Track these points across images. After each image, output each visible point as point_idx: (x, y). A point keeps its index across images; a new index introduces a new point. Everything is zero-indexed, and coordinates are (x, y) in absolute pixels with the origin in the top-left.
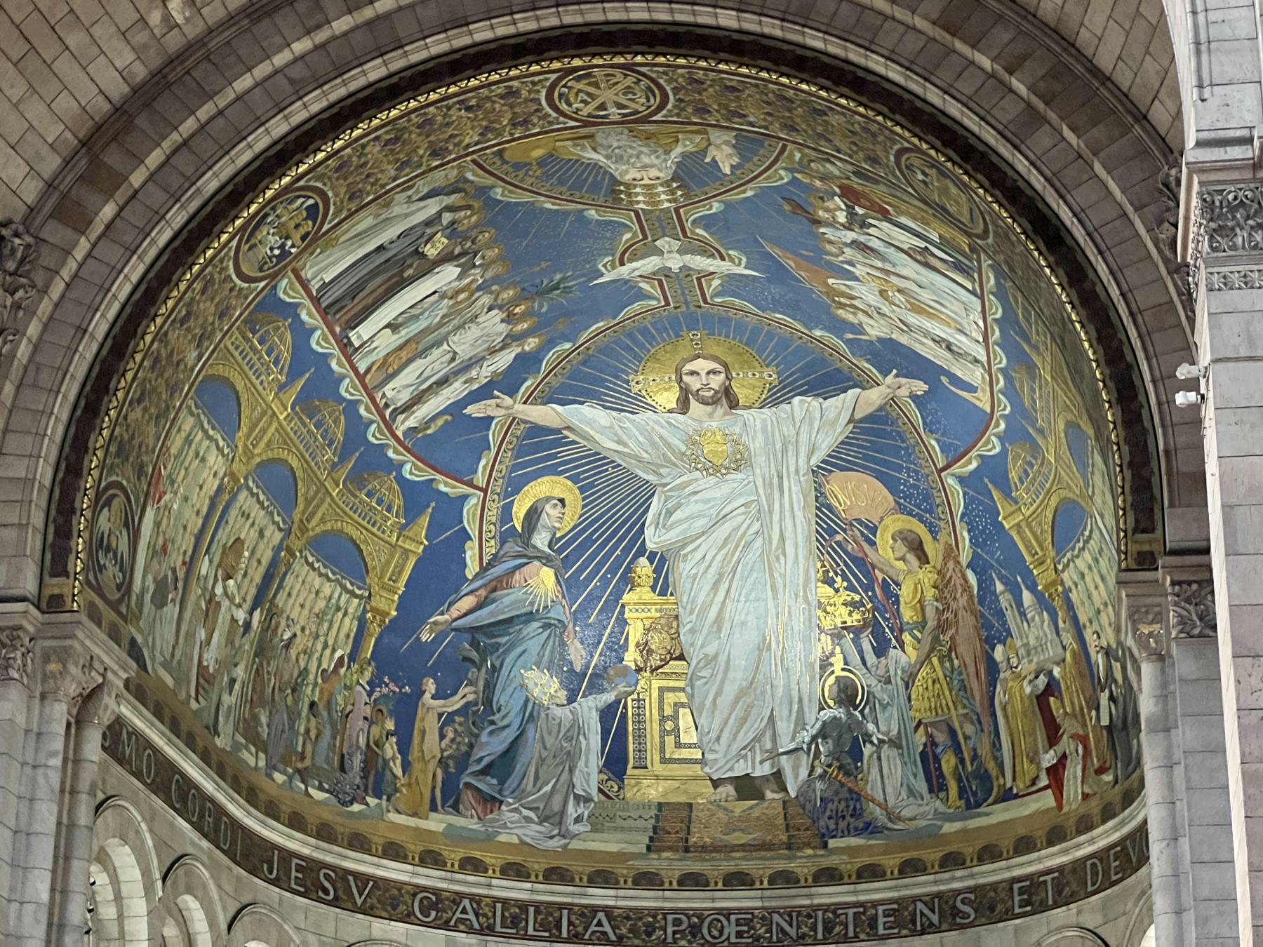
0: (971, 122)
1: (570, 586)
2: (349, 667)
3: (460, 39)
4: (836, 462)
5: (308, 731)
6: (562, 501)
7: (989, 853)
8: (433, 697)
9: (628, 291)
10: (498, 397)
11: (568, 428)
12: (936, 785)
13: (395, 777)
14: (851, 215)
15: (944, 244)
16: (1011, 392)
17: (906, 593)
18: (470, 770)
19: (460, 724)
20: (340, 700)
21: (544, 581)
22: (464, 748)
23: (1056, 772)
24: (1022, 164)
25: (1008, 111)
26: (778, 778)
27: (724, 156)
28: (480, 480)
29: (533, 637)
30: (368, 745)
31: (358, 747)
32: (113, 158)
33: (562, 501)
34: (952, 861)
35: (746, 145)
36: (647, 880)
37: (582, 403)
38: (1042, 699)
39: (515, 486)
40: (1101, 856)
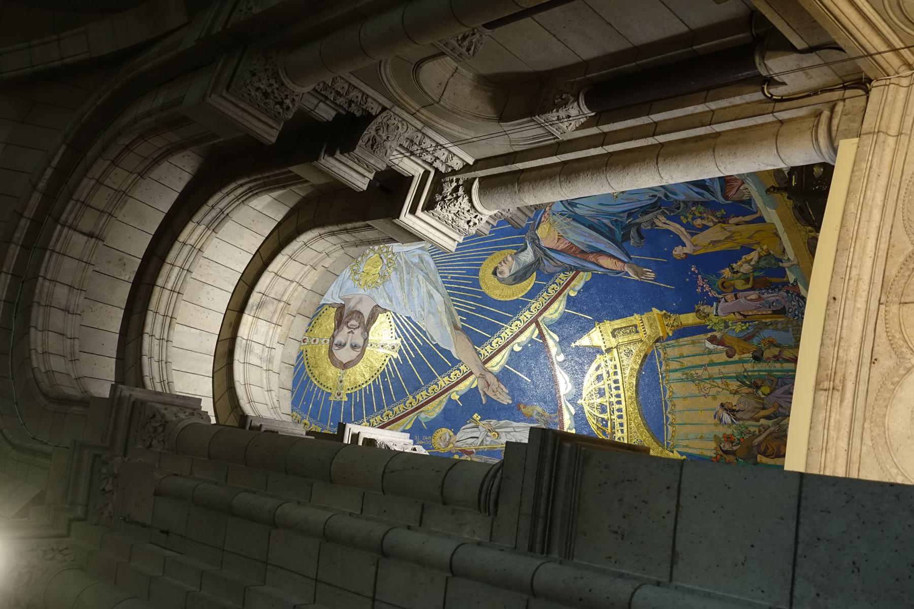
2: (712, 330)
5: (777, 358)
6: (495, 273)
8: (684, 245)
10: (485, 394)
11: (456, 327)
13: (760, 257)
18: (713, 199)
19: (686, 217)
20: (738, 328)
22: (702, 209)
28: (531, 333)
30: (752, 289)
31: (760, 298)
33: (495, 273)
37: (437, 346)
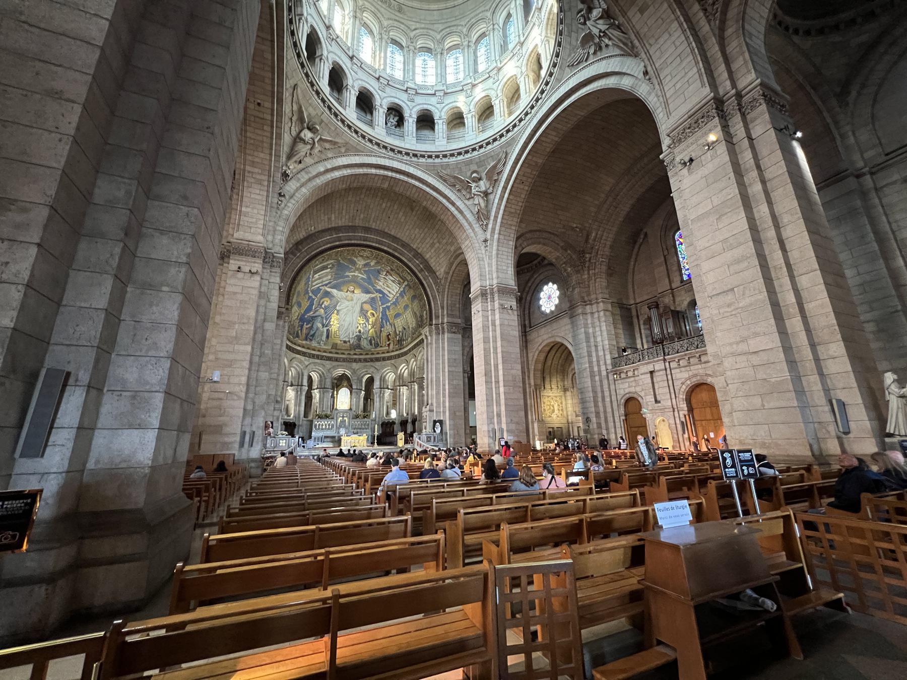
0: (414, 269)
1: (326, 313)
3: (350, 242)
4: (364, 302)
7: (378, 353)
9: (348, 276)
12: (371, 344)
14: (386, 275)
15: (399, 281)
16: (397, 299)
17: (370, 320)
21: (322, 311)
23: (389, 345)
24: (420, 275)
25: (419, 268)
26: (349, 341)
27: (372, 264)
29: (319, 319)
32: (300, 247)
34: (372, 354)
35: (376, 263)
36: (330, 352)
38: (388, 336)
39: (322, 298)
40: (395, 355)
